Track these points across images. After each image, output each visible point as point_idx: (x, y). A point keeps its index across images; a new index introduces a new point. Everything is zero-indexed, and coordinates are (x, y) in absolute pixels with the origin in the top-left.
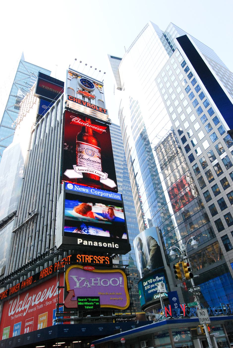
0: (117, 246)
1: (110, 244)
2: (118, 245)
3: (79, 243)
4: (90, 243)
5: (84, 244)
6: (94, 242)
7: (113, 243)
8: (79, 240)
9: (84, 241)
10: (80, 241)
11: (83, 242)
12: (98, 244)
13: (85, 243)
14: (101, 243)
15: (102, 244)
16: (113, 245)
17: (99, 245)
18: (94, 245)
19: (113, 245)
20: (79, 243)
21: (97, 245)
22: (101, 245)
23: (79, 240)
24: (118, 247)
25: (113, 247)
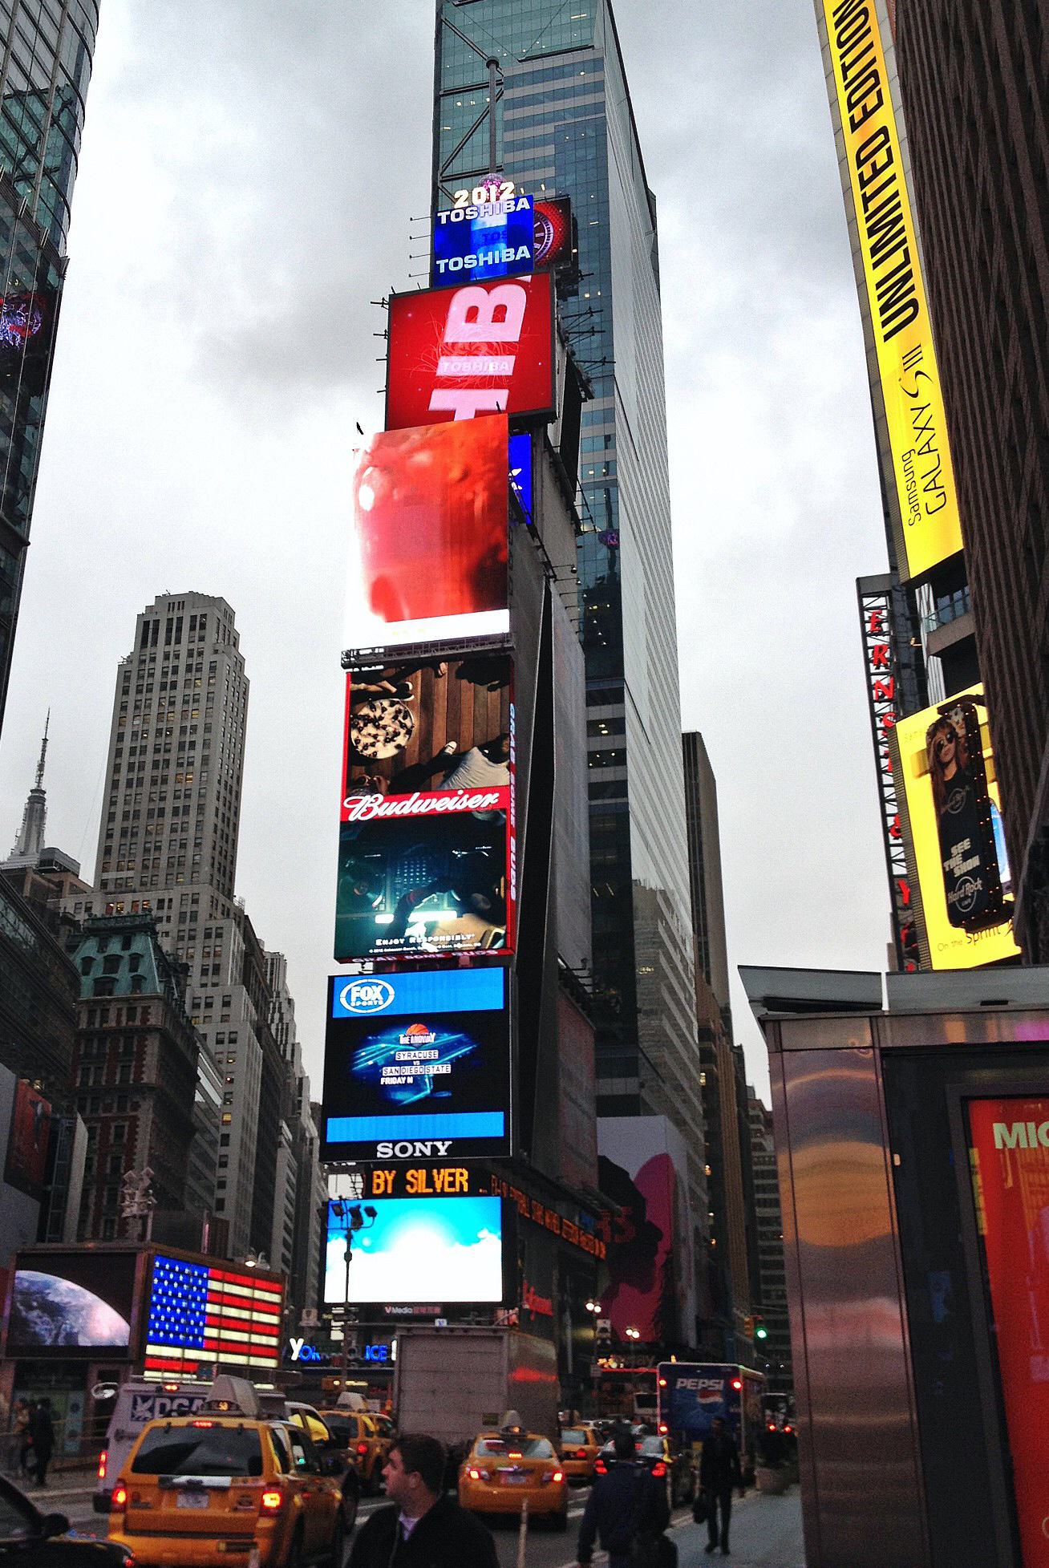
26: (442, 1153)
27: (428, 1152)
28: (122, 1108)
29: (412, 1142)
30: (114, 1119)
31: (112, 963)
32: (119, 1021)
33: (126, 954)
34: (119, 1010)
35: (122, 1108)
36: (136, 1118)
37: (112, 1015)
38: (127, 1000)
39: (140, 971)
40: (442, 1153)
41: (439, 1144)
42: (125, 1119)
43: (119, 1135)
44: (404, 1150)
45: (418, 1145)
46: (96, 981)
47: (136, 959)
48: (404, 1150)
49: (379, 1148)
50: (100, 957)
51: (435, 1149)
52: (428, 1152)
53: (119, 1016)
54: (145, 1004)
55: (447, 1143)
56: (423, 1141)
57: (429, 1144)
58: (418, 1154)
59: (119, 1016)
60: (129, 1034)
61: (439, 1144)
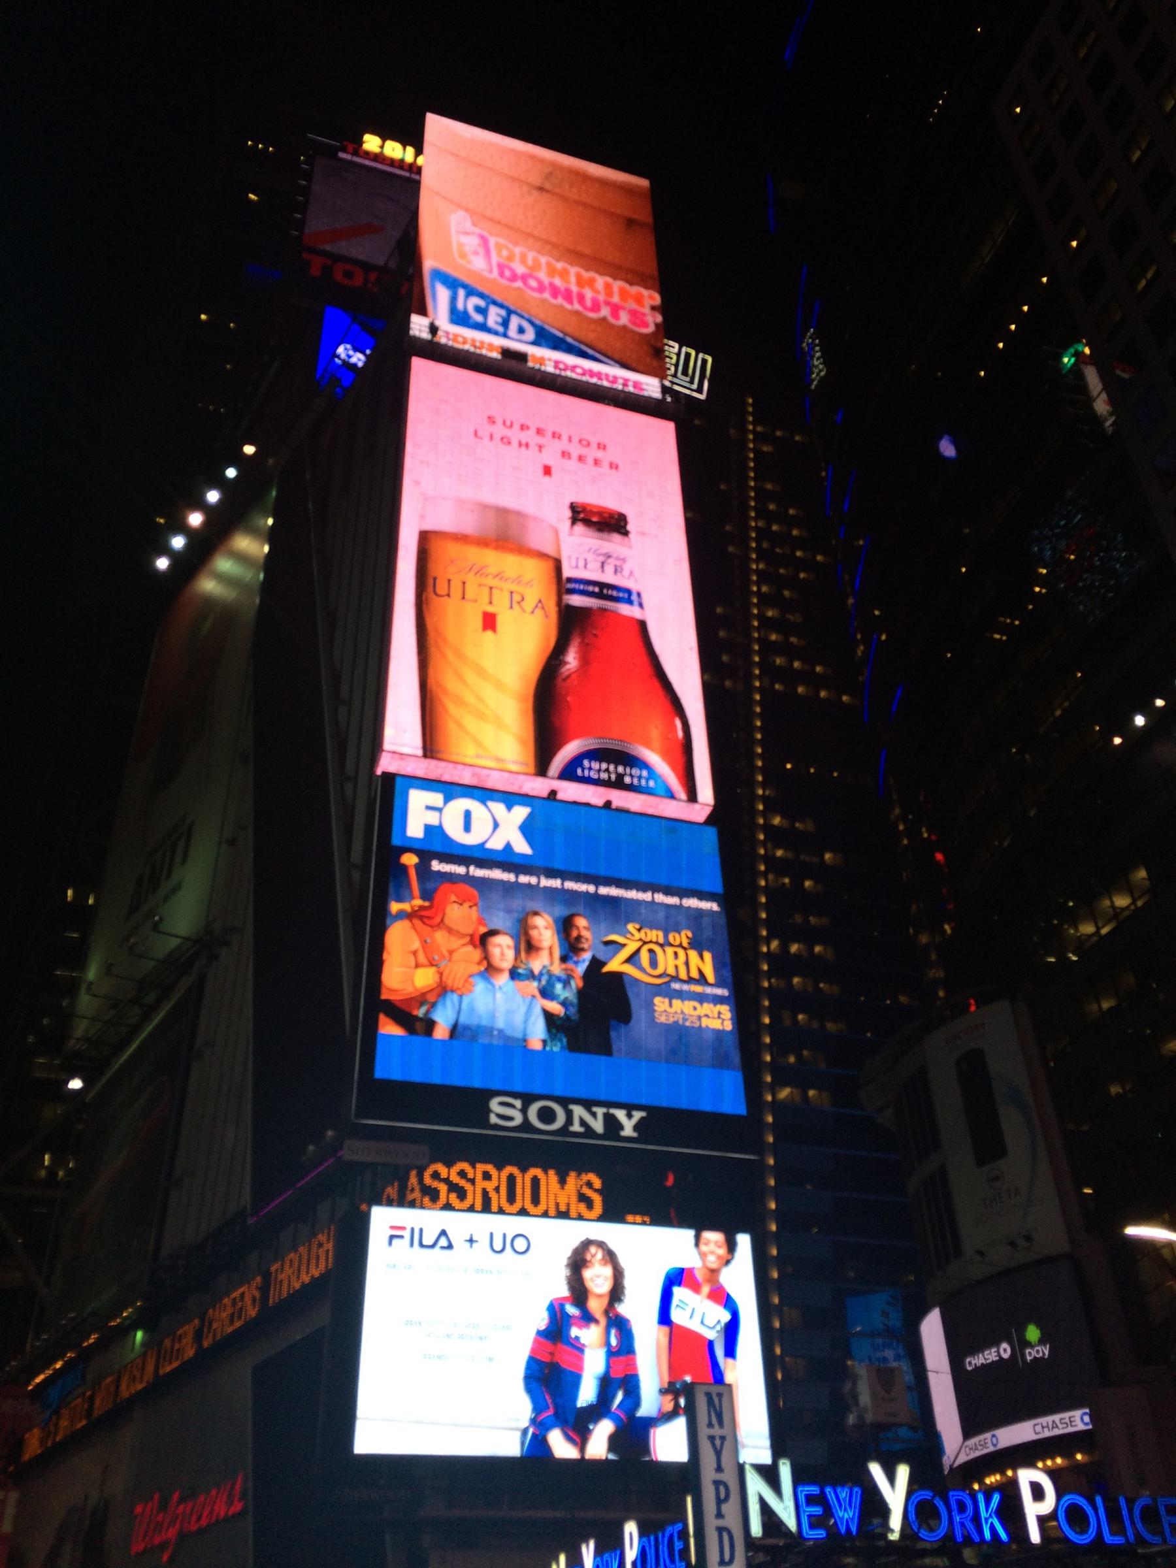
26: (628, 1130)
27: (598, 1126)
29: (564, 1102)
40: (628, 1130)
41: (620, 1114)
44: (547, 1115)
45: (578, 1111)
48: (547, 1115)
49: (494, 1104)
51: (612, 1124)
52: (598, 1126)
55: (638, 1115)
56: (588, 1104)
57: (600, 1111)
58: (576, 1127)
61: (620, 1114)
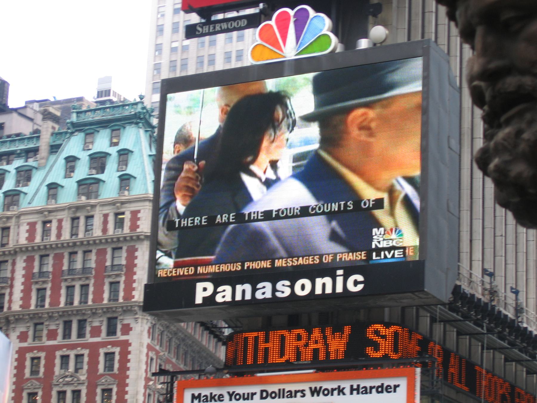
0: (356, 283)
1: (328, 281)
2: (360, 278)
3: (199, 300)
4: (244, 292)
5: (219, 299)
6: (260, 285)
7: (340, 272)
8: (200, 286)
9: (220, 289)
10: (205, 289)
11: (215, 293)
12: (274, 290)
13: (225, 294)
14: (288, 283)
15: (292, 287)
16: (340, 281)
17: (279, 295)
18: (259, 295)
19: (340, 281)
20: (199, 300)
21: (269, 295)
22: (287, 292)
23: (200, 286)
24: (360, 287)
25: (339, 289)
28: (111, 332)
30: (104, 344)
31: (99, 161)
32: (105, 230)
33: (113, 151)
34: (106, 216)
35: (111, 332)
36: (125, 345)
37: (97, 222)
38: (113, 203)
39: (130, 170)
42: (114, 344)
43: (109, 366)
46: (80, 183)
47: (124, 155)
50: (84, 157)
53: (105, 222)
54: (134, 207)
59: (105, 222)
60: (116, 245)
